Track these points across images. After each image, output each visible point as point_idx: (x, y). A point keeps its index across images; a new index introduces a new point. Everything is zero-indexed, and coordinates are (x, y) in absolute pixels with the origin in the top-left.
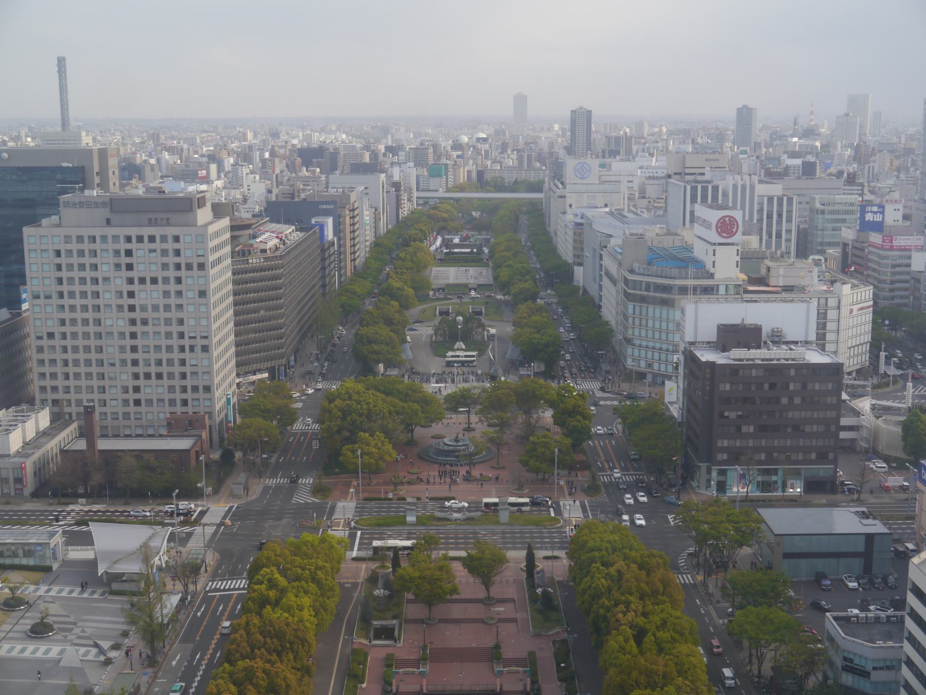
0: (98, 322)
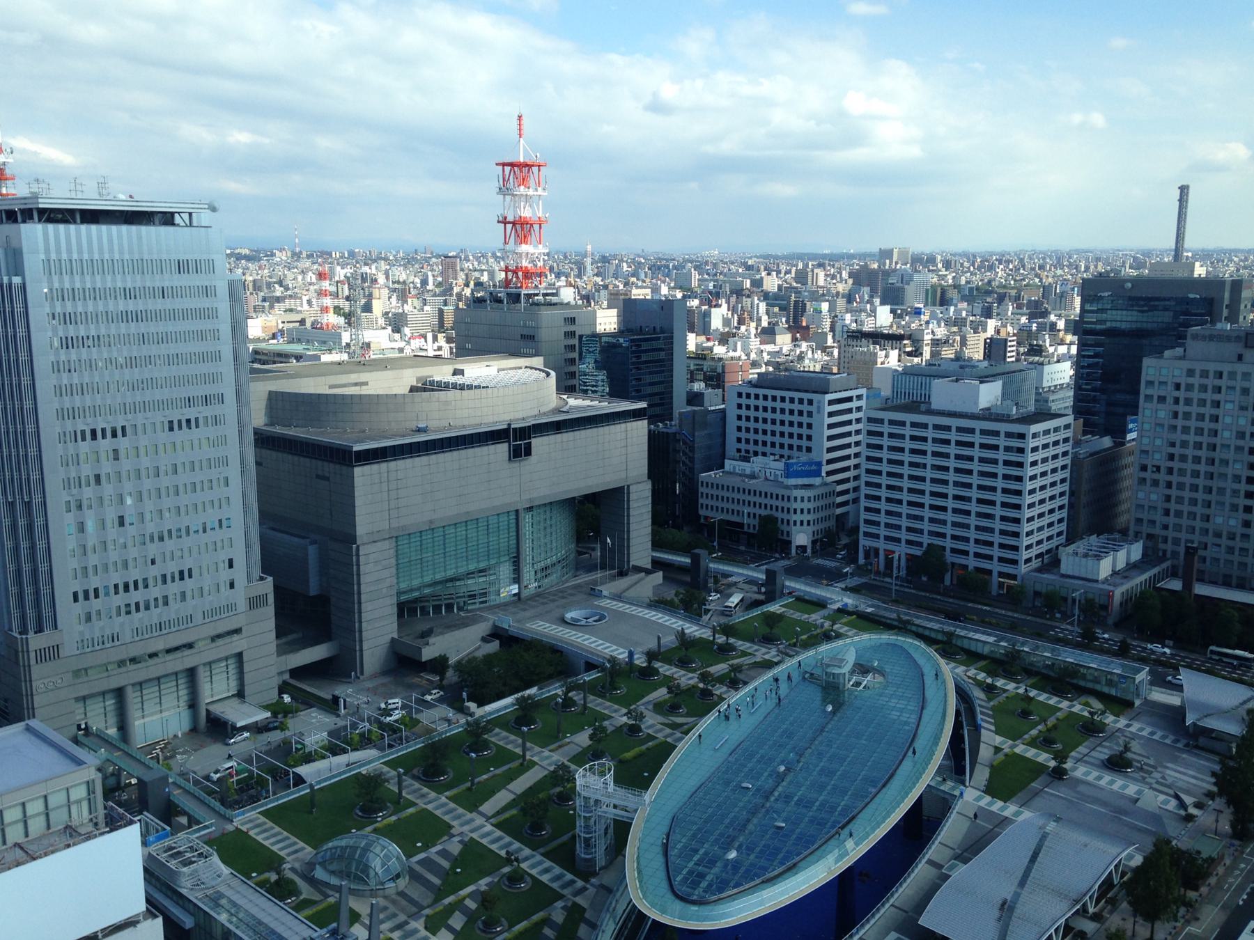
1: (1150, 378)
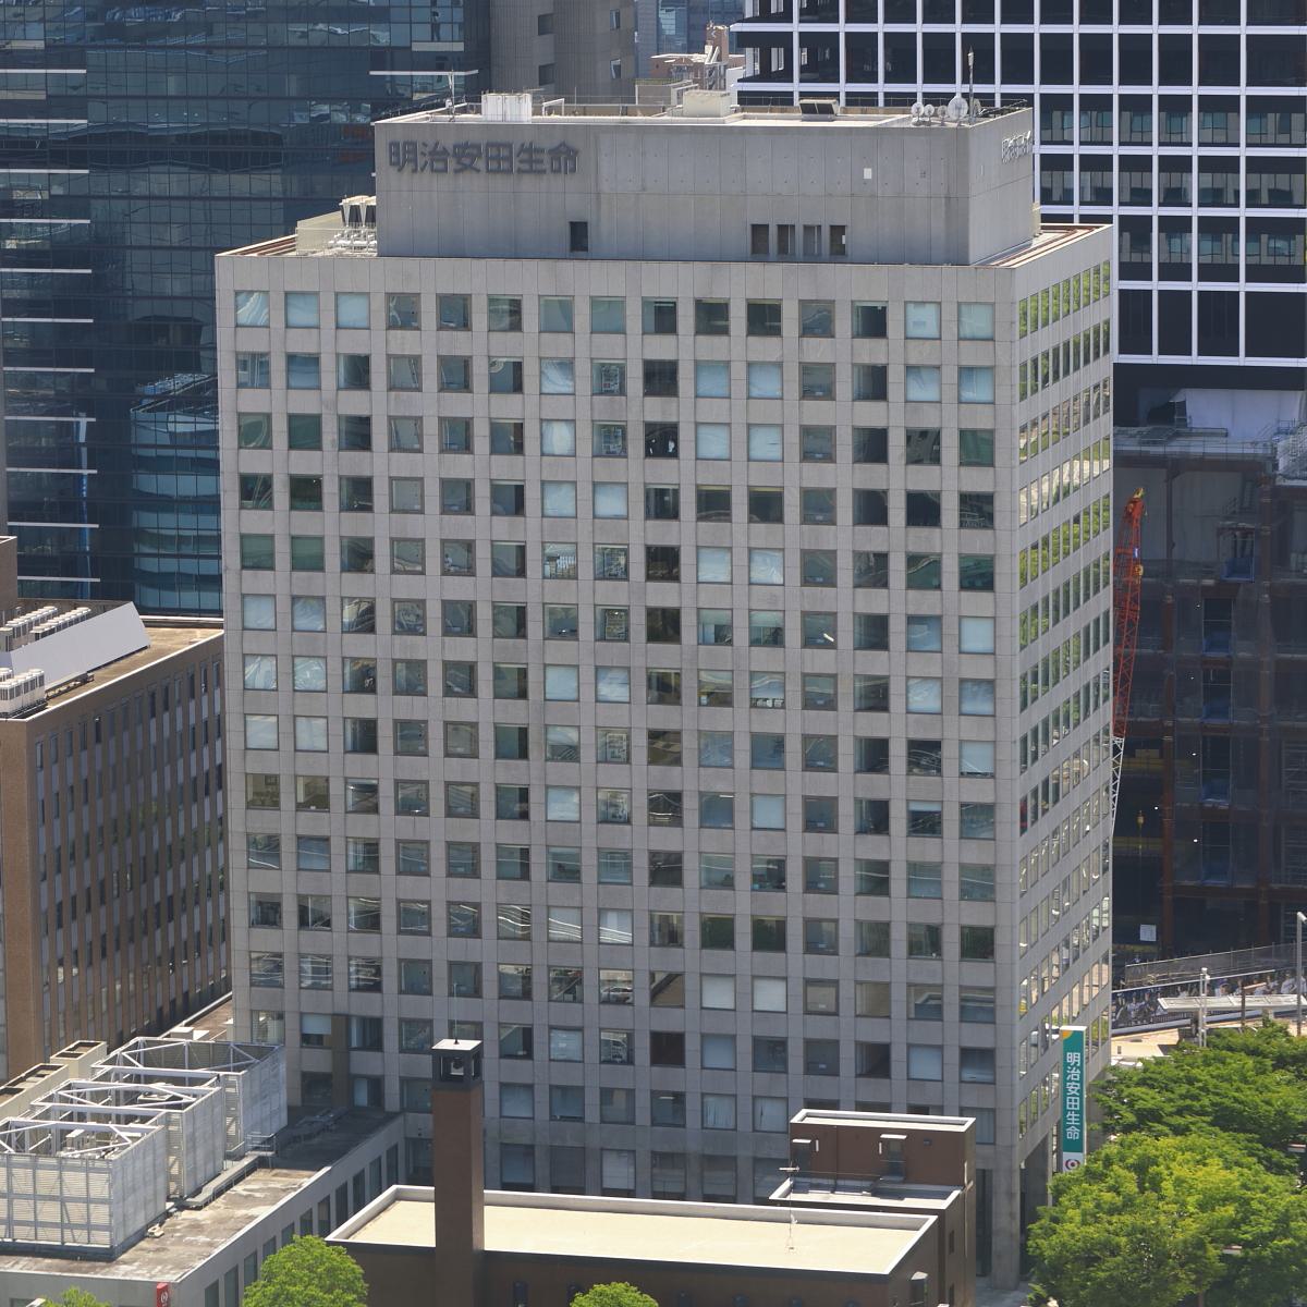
0: (516, 685)
1: (253, 343)
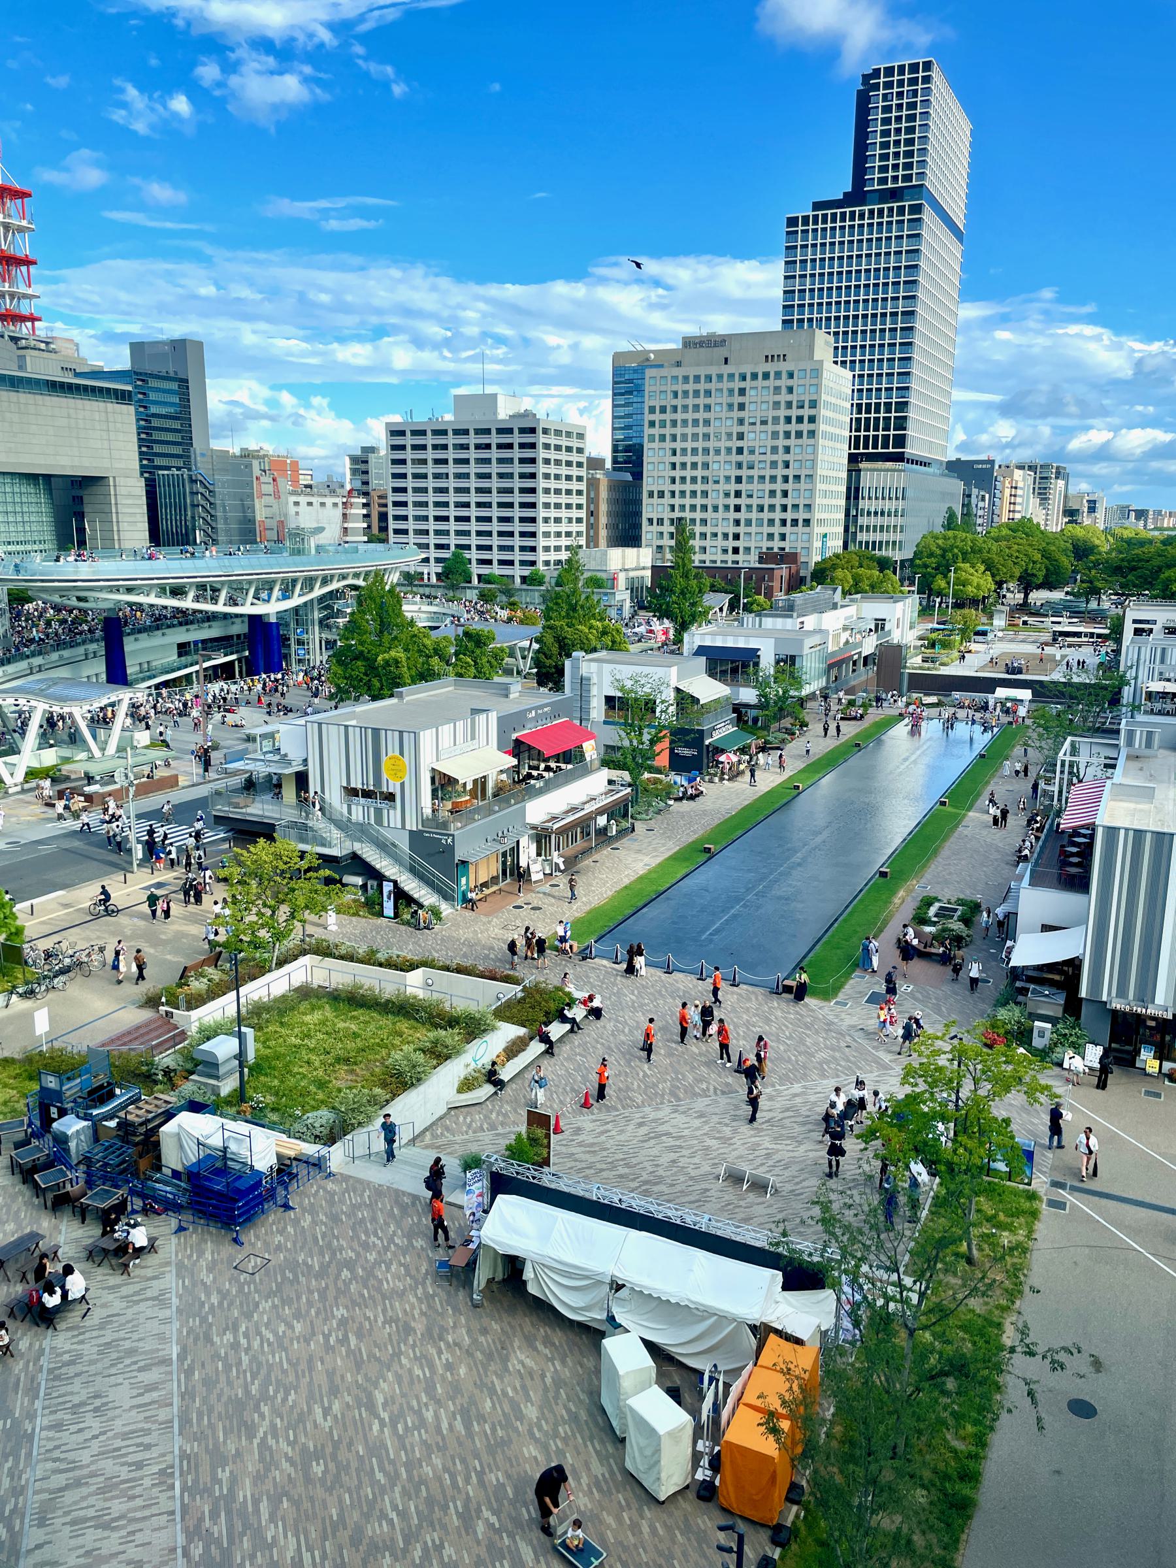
0: (706, 466)
